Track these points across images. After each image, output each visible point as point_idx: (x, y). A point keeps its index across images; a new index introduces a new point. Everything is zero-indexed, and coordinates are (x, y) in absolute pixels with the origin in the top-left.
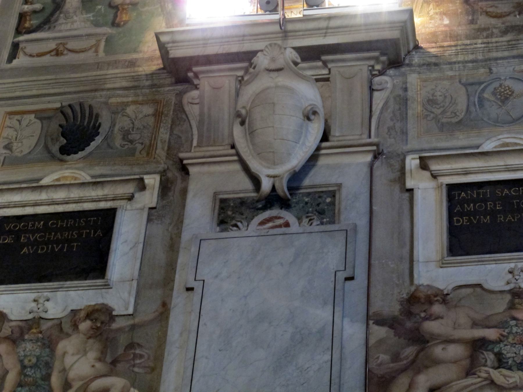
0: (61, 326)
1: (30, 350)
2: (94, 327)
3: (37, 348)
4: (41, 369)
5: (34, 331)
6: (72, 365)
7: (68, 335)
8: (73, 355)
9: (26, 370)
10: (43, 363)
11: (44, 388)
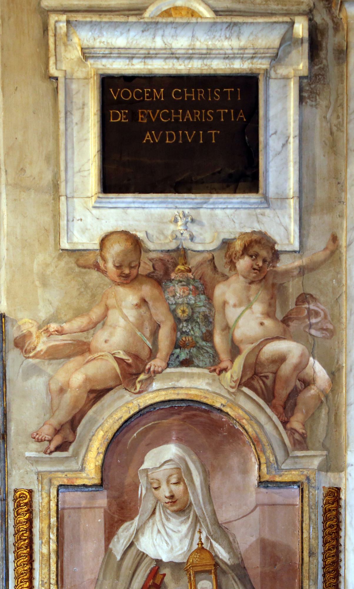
0: (214, 263)
2: (256, 267)
3: (189, 294)
5: (180, 267)
6: (237, 321)
7: (225, 278)
8: (235, 306)
9: (181, 325)
10: (201, 316)
11: (208, 352)
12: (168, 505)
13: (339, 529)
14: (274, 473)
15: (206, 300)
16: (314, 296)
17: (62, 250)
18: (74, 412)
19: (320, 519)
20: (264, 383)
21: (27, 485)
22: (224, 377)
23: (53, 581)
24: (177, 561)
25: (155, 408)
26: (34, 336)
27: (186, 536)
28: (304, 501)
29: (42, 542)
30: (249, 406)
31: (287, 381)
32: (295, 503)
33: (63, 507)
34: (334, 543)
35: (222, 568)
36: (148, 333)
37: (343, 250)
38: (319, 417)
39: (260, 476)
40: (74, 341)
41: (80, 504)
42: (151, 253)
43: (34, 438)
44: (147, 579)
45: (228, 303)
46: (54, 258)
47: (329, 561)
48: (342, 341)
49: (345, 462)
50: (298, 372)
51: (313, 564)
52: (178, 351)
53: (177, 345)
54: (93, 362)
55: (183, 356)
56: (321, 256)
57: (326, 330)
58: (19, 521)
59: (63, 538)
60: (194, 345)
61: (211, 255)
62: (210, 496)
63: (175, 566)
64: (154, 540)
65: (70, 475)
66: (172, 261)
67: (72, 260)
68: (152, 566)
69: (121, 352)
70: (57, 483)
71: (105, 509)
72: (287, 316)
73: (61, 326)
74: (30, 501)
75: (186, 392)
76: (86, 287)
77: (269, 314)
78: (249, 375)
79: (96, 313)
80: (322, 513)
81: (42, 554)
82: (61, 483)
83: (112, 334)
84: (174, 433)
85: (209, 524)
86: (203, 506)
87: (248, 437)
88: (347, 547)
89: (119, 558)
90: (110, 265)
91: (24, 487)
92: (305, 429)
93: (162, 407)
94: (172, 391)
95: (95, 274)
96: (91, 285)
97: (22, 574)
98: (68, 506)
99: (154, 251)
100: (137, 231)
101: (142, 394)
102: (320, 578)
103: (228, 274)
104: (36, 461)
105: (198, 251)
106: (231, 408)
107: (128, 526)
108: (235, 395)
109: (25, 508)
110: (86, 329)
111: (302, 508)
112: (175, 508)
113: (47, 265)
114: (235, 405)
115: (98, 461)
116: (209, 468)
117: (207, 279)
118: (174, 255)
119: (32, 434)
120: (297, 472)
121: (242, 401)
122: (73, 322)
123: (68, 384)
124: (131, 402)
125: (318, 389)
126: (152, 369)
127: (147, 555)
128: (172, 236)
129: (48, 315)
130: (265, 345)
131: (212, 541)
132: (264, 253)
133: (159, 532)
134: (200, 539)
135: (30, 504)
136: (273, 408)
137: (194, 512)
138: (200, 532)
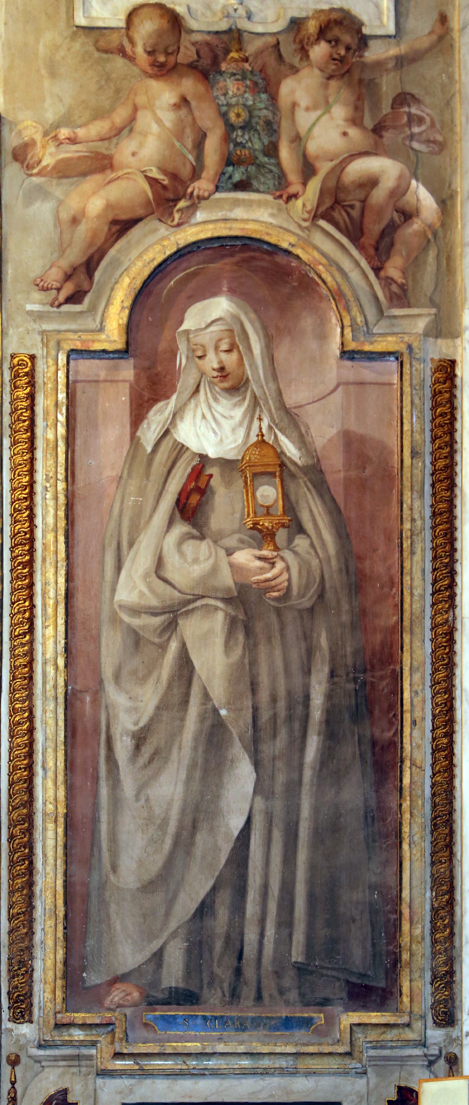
0: (279, 50)
1: (235, 95)
2: (336, 56)
3: (245, 92)
4: (259, 134)
5: (234, 55)
6: (310, 129)
7: (295, 70)
8: (307, 109)
9: (235, 133)
10: (261, 122)
11: (271, 171)
12: (216, 380)
13: (453, 419)
14: (362, 339)
15: (268, 100)
16: (417, 96)
17: (77, 27)
18: (91, 251)
19: (428, 404)
20: (348, 214)
21: (28, 349)
22: (294, 206)
23: (61, 476)
24: (228, 457)
25: (199, 247)
26: (39, 145)
27: (241, 424)
28: (404, 379)
29: (47, 425)
30: (328, 247)
31: (380, 212)
32: (392, 382)
33: (74, 379)
34: (447, 439)
35: (289, 471)
36: (189, 143)
37: (456, 35)
38: (425, 262)
39: (342, 344)
40: (91, 152)
41: (98, 375)
42: (194, 35)
43: (38, 285)
44: (187, 480)
45: (299, 105)
46: (66, 38)
47: (441, 463)
48: (456, 158)
49: (460, 324)
50: (395, 199)
51: (417, 468)
52: (230, 169)
53: (229, 161)
54: (115, 183)
55: (237, 177)
56: (425, 43)
57: (434, 142)
58: (17, 396)
59: (75, 420)
60: (252, 161)
61: (275, 39)
62: (274, 369)
64: (198, 428)
65: (84, 336)
66: (223, 45)
67: (90, 41)
68: (194, 463)
69: (154, 169)
70: (67, 346)
71: (130, 384)
72: (379, 123)
73: (74, 132)
74: (31, 370)
75: (242, 226)
76: (108, 79)
77: (355, 121)
78: (328, 203)
79: (120, 115)
80: (430, 396)
81: (47, 440)
82: (72, 347)
83: (141, 145)
84: (225, 282)
85: (273, 408)
86: (264, 383)
87: (326, 289)
88: (464, 446)
89: (149, 449)
90: (140, 50)
91: (23, 352)
92: (405, 278)
93: (208, 246)
94: (222, 225)
95: (119, 62)
96: (114, 76)
97: (21, 465)
98: (82, 379)
99: (198, 31)
100: (175, 5)
101: (182, 227)
102: (428, 489)
103: (297, 65)
104: (40, 316)
105: (258, 34)
106: (303, 249)
107: (162, 407)
108: (309, 231)
109: (25, 380)
110: (107, 136)
111: (402, 389)
112: (226, 385)
113: (57, 47)
114: (308, 243)
115: (122, 319)
116: (272, 331)
117: (270, 71)
118: (225, 38)
119: (35, 280)
120: (395, 339)
121: (318, 239)
122: (91, 126)
123: (83, 212)
125: (423, 222)
126: (195, 194)
127: (187, 449)
128: (223, 13)
129: (57, 117)
130: (349, 163)
131: (276, 431)
132: (347, 38)
133: (204, 417)
134: (261, 429)
135: (31, 375)
136: (361, 248)
137: (252, 390)
138: (260, 419)
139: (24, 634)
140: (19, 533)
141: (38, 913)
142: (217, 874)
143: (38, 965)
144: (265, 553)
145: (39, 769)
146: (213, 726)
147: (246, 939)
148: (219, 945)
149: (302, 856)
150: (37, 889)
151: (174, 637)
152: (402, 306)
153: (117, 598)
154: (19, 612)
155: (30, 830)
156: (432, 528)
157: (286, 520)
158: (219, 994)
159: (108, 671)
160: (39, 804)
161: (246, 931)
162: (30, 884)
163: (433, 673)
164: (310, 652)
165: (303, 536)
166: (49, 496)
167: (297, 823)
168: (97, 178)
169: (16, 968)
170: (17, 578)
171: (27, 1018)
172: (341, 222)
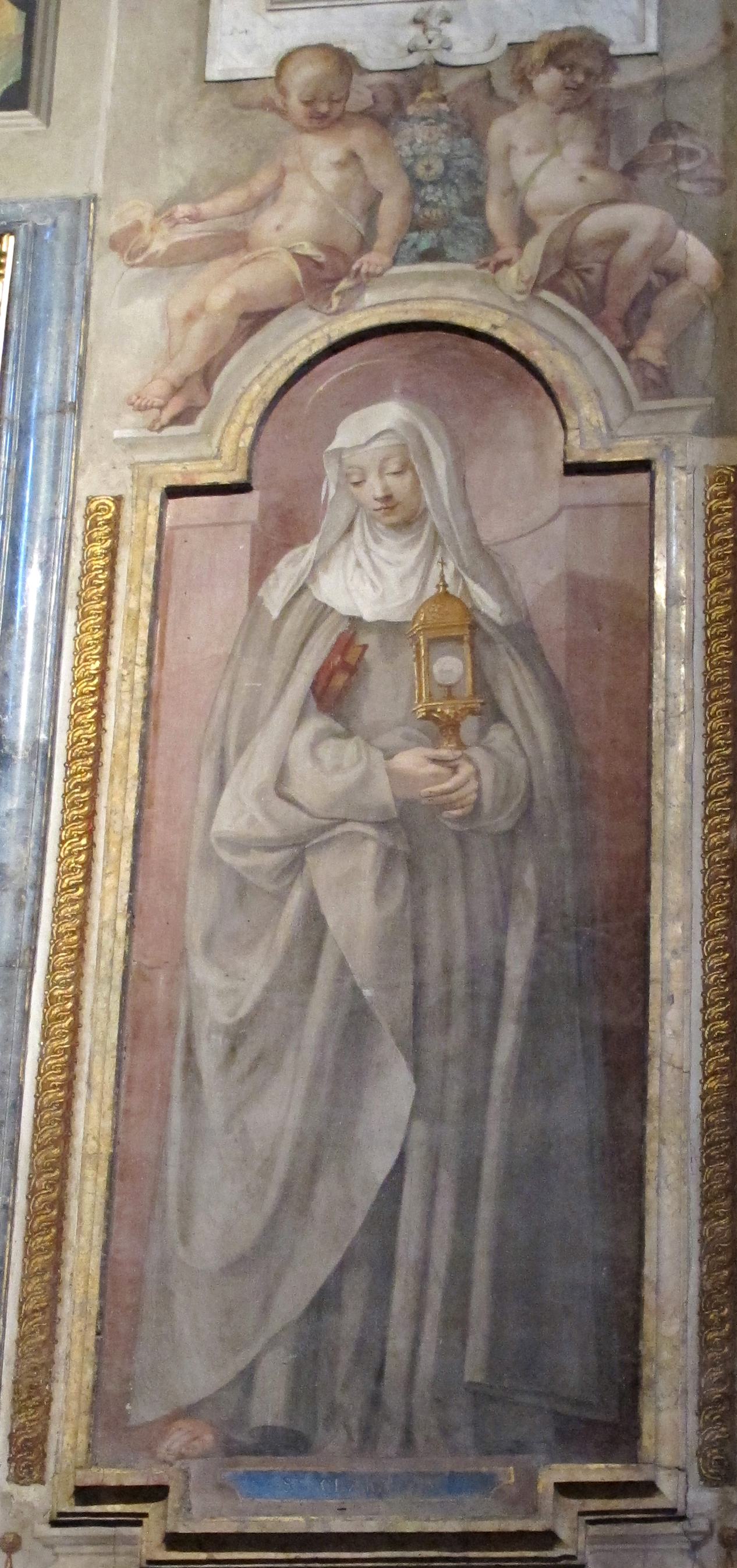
0: (490, 83)
1: (425, 143)
2: (571, 85)
4: (458, 189)
5: (427, 94)
6: (532, 177)
7: (511, 106)
10: (462, 174)
11: (473, 234)
12: (378, 514)
26: (147, 226)
27: (414, 570)
43: (132, 404)
45: (516, 148)
52: (415, 235)
53: (416, 226)
55: (424, 245)
59: (169, 580)
63: (389, 629)
68: (340, 630)
69: (306, 245)
71: (253, 526)
72: (631, 162)
77: (596, 162)
79: (263, 180)
86: (450, 514)
89: (275, 614)
97: (89, 646)
104: (131, 445)
109: (106, 529)
112: (393, 519)
119: (129, 398)
121: (539, 315)
124: (320, 328)
126: (363, 270)
127: (333, 610)
131: (466, 578)
133: (358, 564)
134: (442, 577)
135: (114, 523)
136: (603, 325)
137: (433, 525)
138: (443, 564)
139: (76, 886)
140: (79, 740)
141: (65, 1310)
142: (346, 1244)
143: (59, 1391)
144: (444, 753)
145: (81, 1087)
146: (352, 1013)
147: (390, 1346)
148: (345, 1356)
149: (486, 1212)
150: (66, 1274)
151: (298, 883)
152: (664, 397)
153: (215, 828)
154: (71, 854)
155: (61, 1182)
156: (706, 705)
157: (477, 703)
158: (342, 1435)
159: (195, 938)
160: (77, 1142)
161: (391, 1333)
162: (57, 1265)
163: (706, 921)
164: (508, 893)
165: (501, 725)
166: (126, 686)
167: (479, 1161)
168: (227, 261)
169: (25, 1396)
170: (73, 805)
171: (36, 1475)
172: (574, 293)
